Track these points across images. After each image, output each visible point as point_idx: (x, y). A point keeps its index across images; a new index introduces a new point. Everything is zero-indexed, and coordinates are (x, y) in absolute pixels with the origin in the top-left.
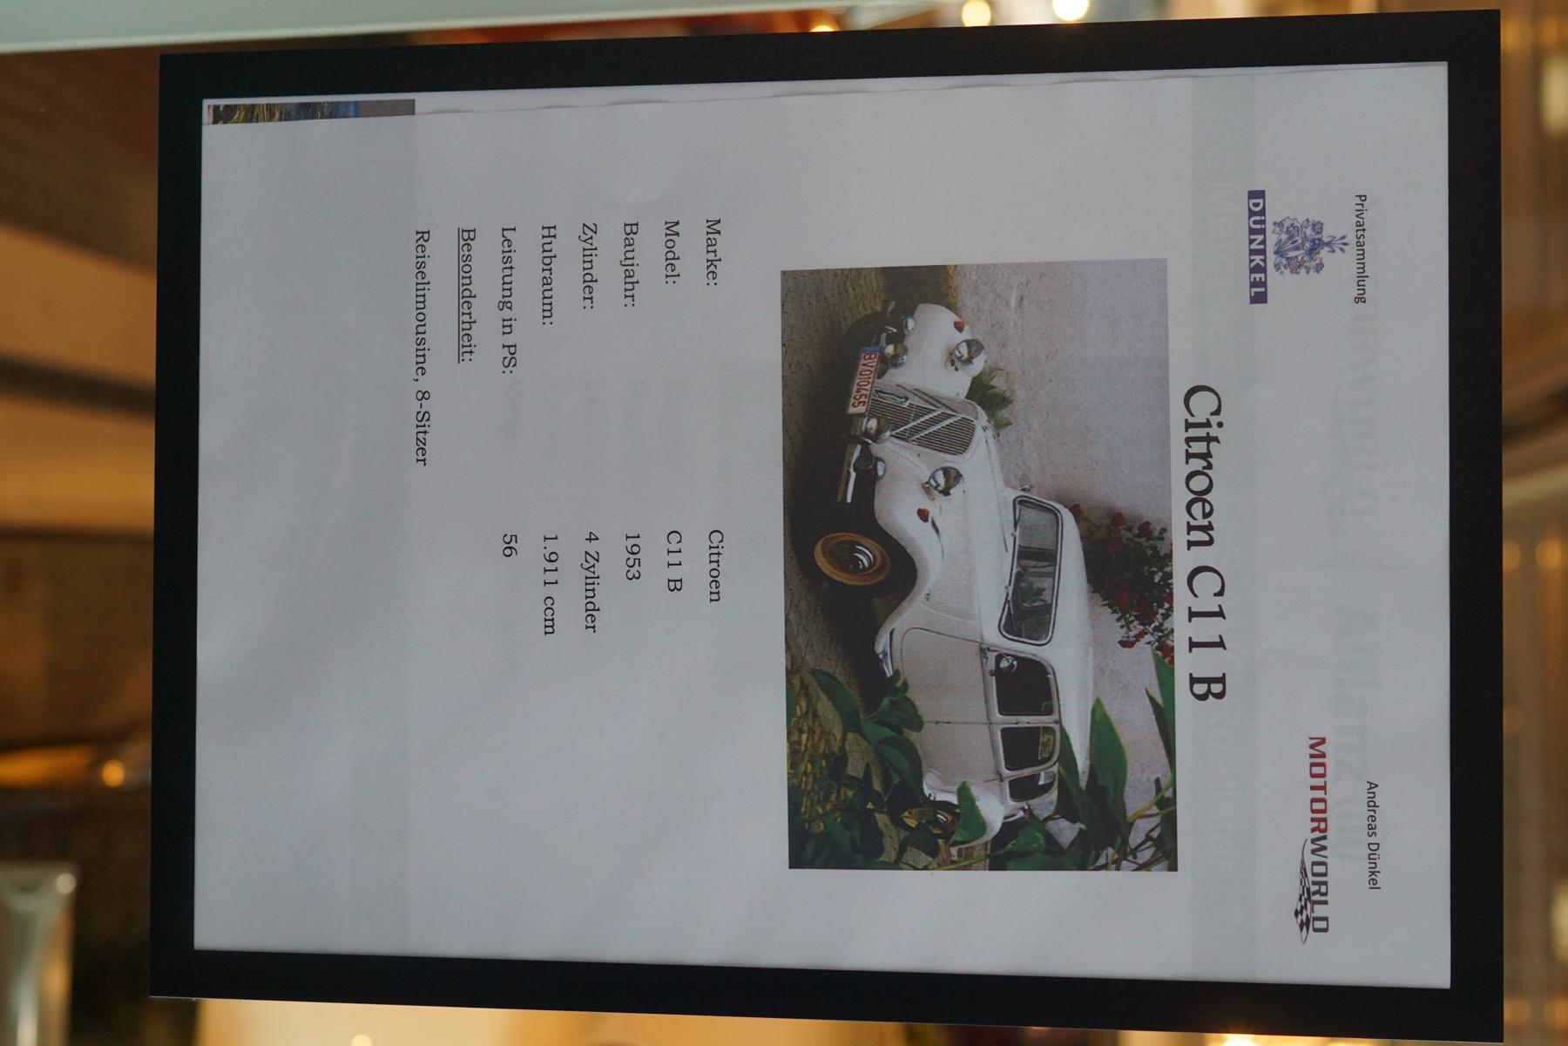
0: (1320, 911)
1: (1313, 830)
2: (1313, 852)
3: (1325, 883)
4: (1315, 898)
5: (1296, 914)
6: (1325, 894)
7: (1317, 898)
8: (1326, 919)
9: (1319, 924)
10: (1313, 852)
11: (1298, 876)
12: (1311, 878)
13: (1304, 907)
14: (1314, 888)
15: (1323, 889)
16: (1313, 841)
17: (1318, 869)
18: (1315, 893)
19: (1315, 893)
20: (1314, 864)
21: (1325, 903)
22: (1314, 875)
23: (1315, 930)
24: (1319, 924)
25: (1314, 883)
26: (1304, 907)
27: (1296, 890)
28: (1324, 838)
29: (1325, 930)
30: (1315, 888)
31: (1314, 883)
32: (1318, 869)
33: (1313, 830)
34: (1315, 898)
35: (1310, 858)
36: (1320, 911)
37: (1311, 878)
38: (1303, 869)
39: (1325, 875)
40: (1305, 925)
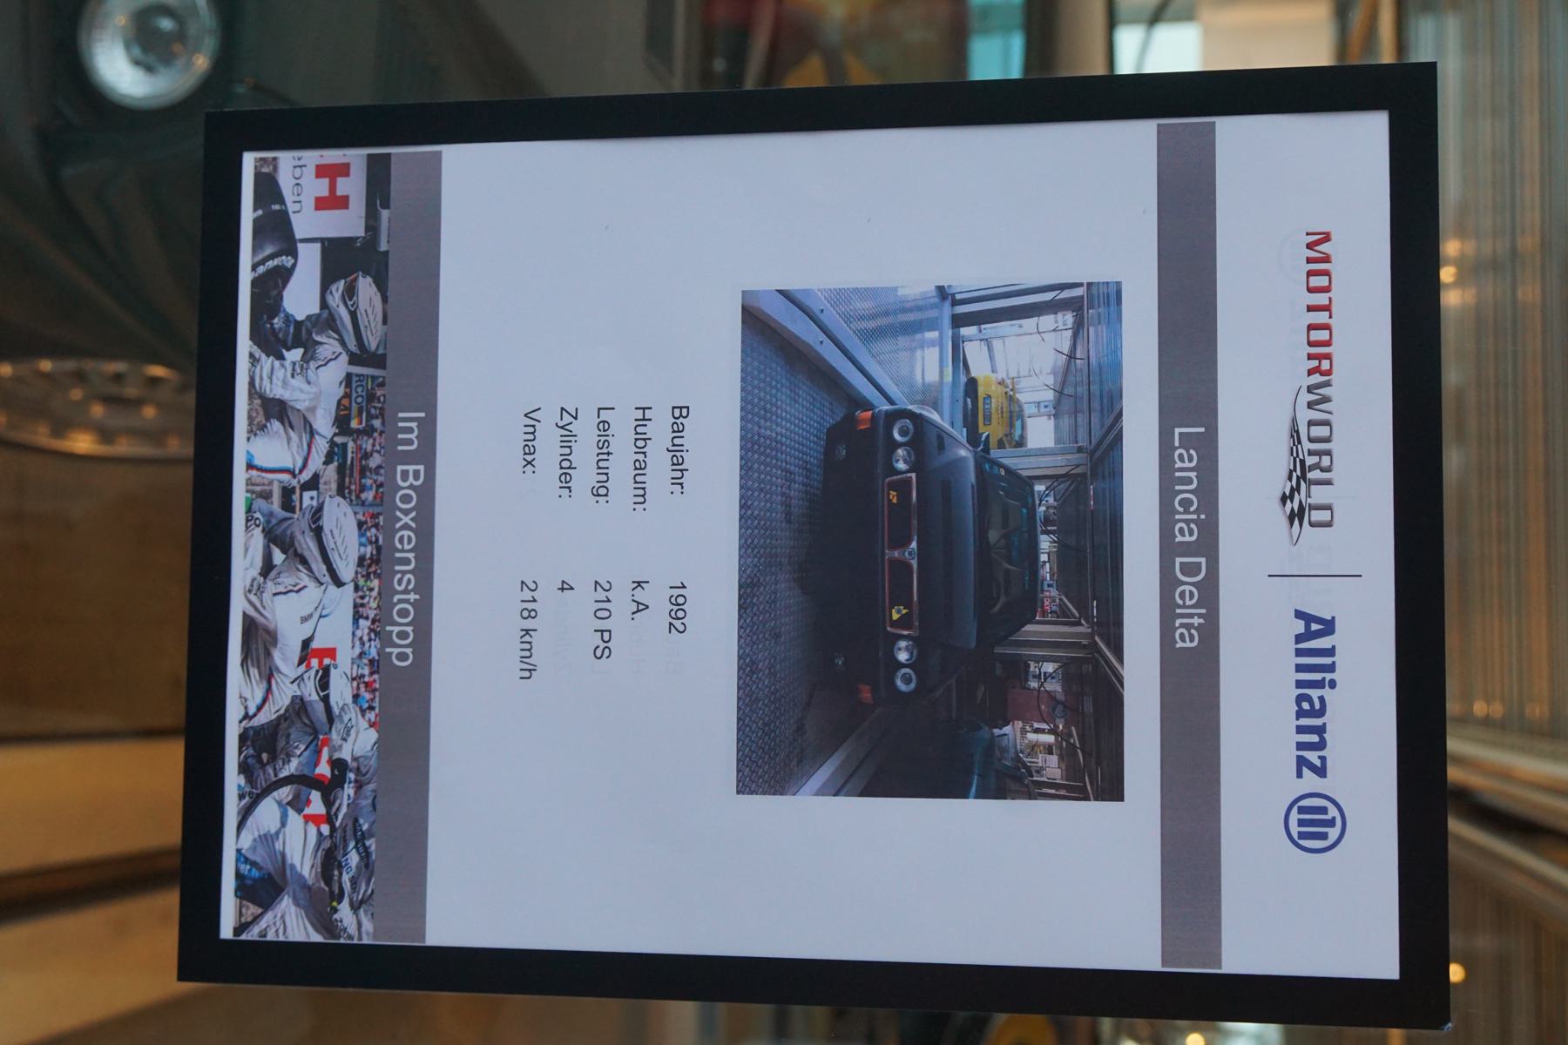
0: (1319, 495)
1: (1310, 372)
2: (1310, 405)
3: (1328, 453)
4: (1310, 475)
5: (1284, 499)
6: (1328, 470)
7: (1314, 475)
8: (1329, 507)
9: (1318, 516)
10: (1310, 405)
11: (1284, 442)
12: (1307, 445)
13: (1295, 490)
14: (1310, 460)
15: (1326, 461)
16: (1310, 390)
17: (1318, 431)
18: (1317, 466)
19: (1312, 468)
20: (1311, 423)
21: (1329, 483)
22: (1311, 440)
23: (1312, 524)
24: (1318, 516)
25: (1311, 453)
26: (1295, 490)
27: (1283, 463)
28: (1328, 384)
29: (1329, 524)
30: (1315, 459)
31: (1311, 453)
32: (1318, 431)
33: (1310, 372)
34: (1314, 475)
35: (1304, 415)
36: (1319, 495)
37: (1307, 445)
38: (1295, 434)
39: (1328, 440)
40: (1296, 516)
